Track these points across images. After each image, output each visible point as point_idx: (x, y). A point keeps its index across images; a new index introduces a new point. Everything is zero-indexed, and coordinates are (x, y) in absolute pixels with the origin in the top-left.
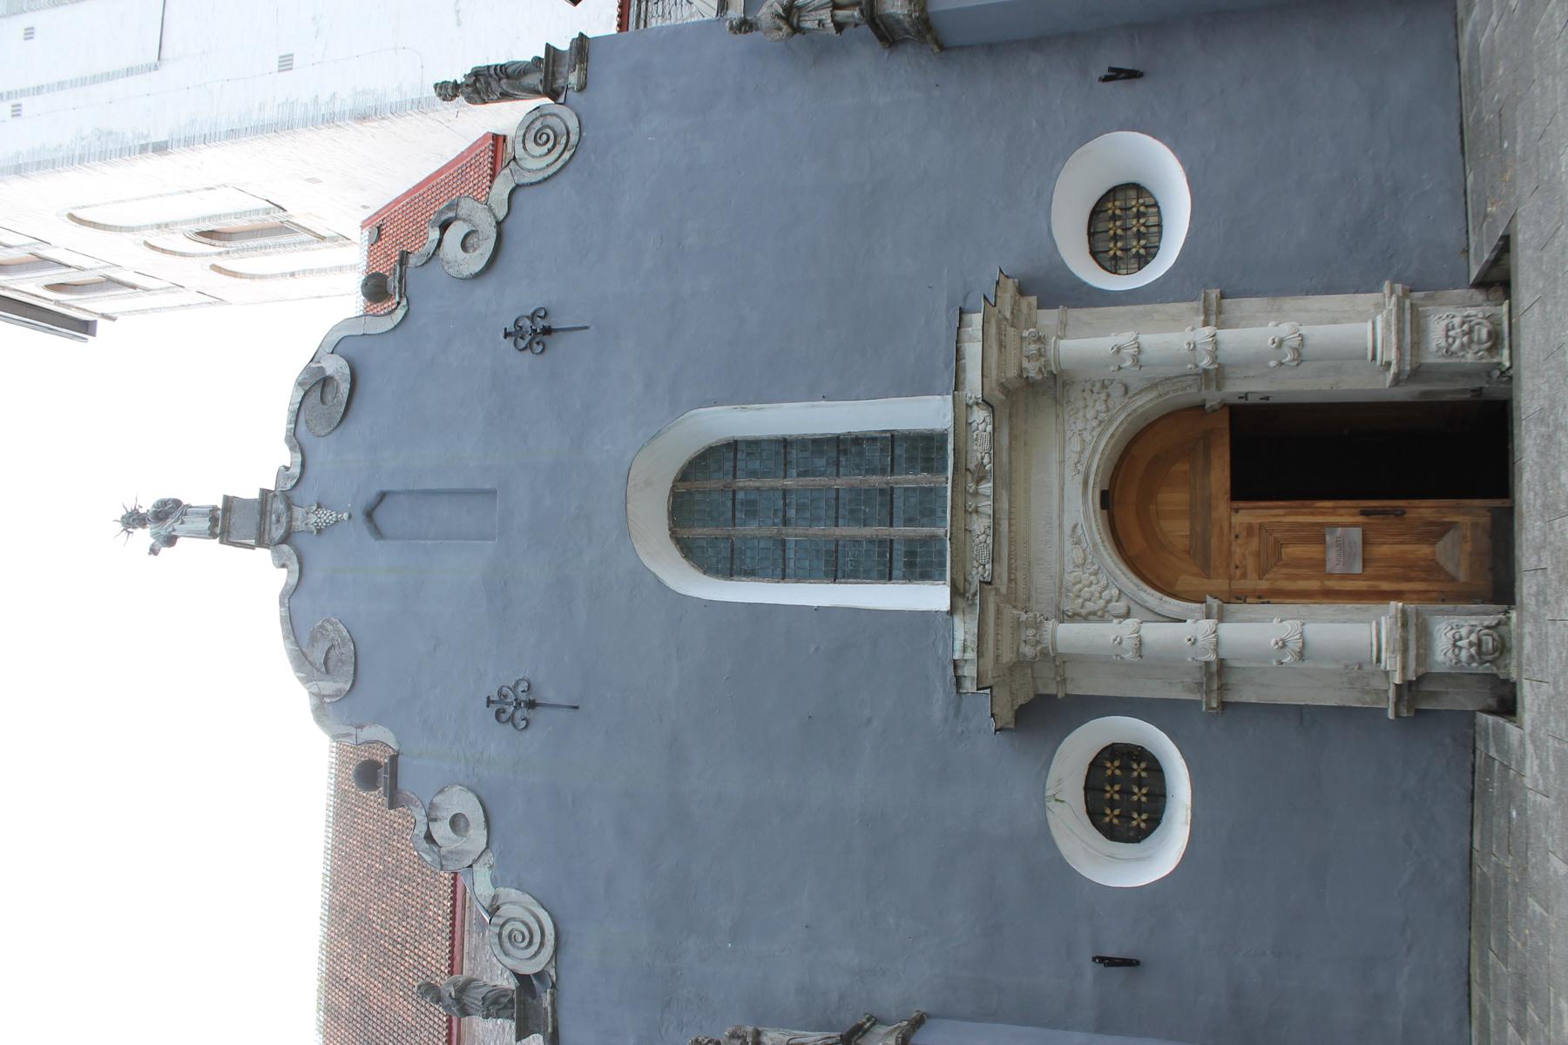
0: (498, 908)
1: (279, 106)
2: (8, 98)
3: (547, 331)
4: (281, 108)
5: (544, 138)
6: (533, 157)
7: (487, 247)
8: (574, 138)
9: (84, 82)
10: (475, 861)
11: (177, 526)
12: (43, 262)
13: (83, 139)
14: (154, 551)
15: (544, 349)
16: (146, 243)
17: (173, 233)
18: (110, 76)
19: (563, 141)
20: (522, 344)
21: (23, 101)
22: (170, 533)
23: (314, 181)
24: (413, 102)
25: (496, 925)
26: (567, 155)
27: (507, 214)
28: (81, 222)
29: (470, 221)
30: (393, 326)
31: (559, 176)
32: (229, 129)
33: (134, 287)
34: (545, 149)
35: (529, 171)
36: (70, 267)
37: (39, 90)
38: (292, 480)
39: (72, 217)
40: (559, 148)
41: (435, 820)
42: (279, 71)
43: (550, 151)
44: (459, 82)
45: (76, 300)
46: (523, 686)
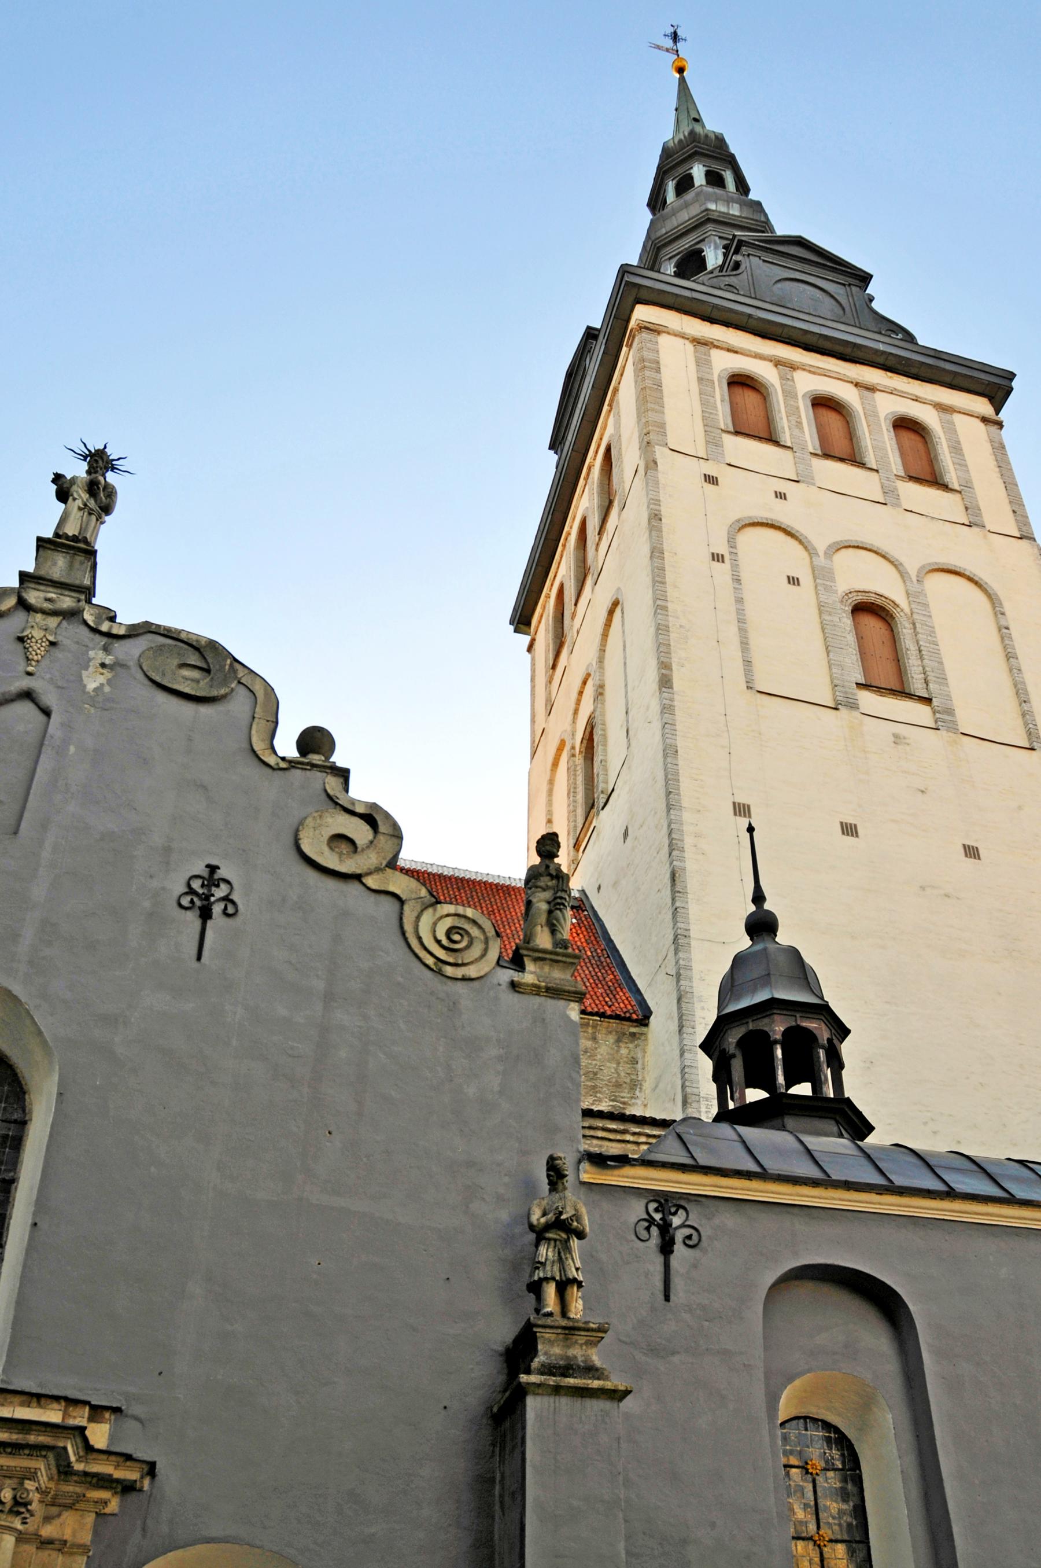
5: (456, 937)
6: (435, 924)
7: (330, 860)
8: (449, 970)
9: (741, 621)
16: (588, 675)
17: (595, 700)
18: (745, 645)
21: (727, 566)
23: (626, 834)
24: (686, 930)
26: (430, 961)
27: (369, 889)
28: (611, 612)
30: (256, 750)
31: (407, 950)
32: (678, 749)
33: (554, 667)
34: (441, 936)
35: (418, 918)
36: (576, 604)
40: (441, 954)
42: (734, 803)
43: (438, 942)
45: (549, 613)
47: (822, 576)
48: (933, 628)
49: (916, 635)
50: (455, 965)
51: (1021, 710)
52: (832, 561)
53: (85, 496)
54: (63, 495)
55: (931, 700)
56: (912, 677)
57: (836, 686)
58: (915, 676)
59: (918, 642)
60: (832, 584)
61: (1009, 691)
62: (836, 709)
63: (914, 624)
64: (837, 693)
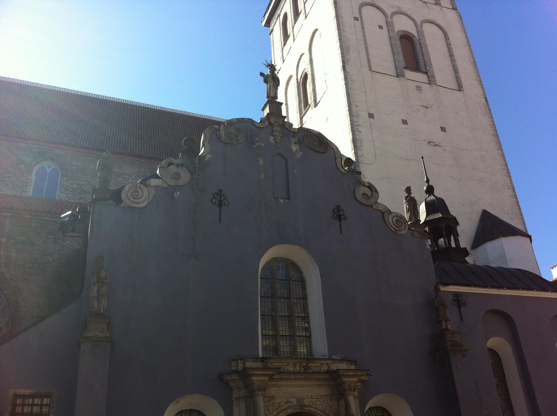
0: (146, 187)
1: (357, 112)
2: (360, 17)
3: (340, 220)
7: (364, 201)
10: (163, 180)
11: (272, 84)
12: (297, 14)
13: (347, 40)
14: (262, 74)
15: (333, 218)
16: (303, 54)
18: (367, 53)
19: (397, 229)
20: (336, 211)
25: (140, 185)
26: (393, 230)
30: (338, 167)
35: (388, 218)
37: (363, 28)
38: (289, 128)
39: (316, 30)
40: (396, 228)
41: (178, 167)
42: (368, 113)
43: (394, 224)
46: (227, 203)
47: (390, 25)
48: (427, 45)
49: (421, 48)
50: (399, 231)
52: (393, 19)
53: (273, 82)
54: (266, 81)
55: (427, 73)
59: (422, 50)
60: (394, 29)
61: (451, 68)
62: (397, 77)
63: (420, 44)
64: (398, 71)
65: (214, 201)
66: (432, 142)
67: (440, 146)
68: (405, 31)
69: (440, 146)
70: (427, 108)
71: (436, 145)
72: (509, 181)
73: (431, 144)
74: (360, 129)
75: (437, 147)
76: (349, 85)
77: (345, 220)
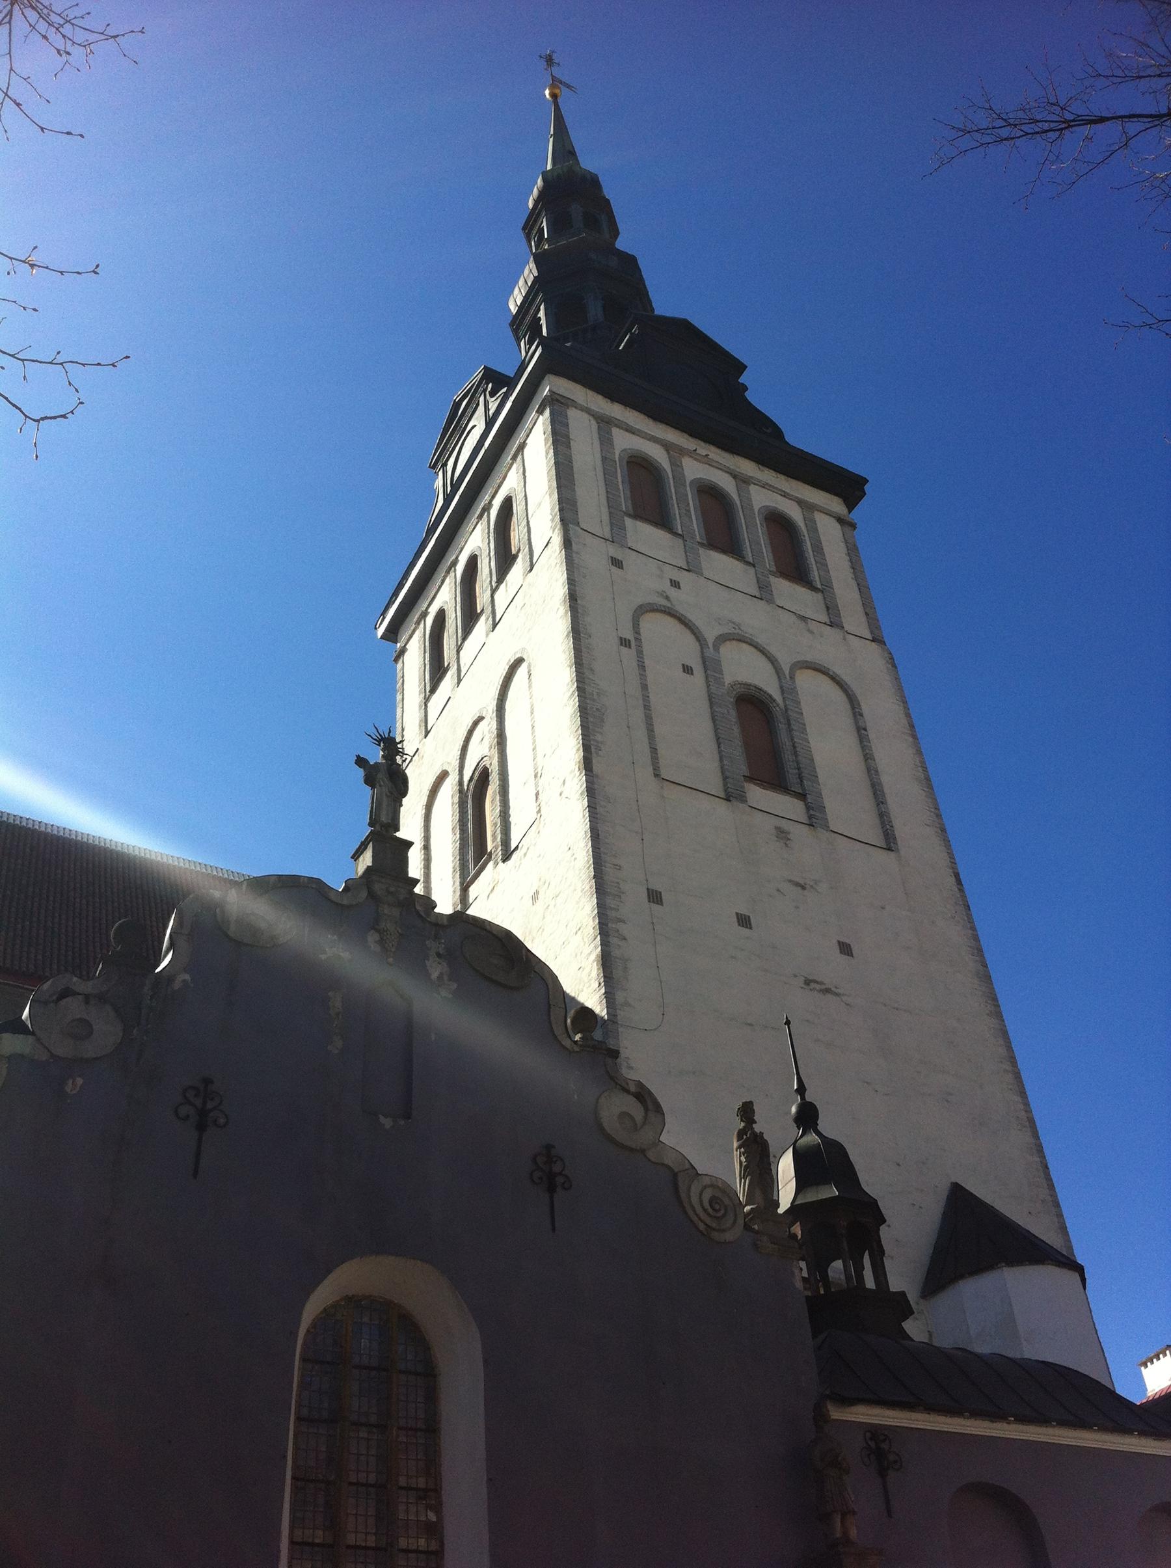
1: (618, 883)
2: (636, 639)
3: (551, 1189)
4: (616, 885)
9: (647, 707)
11: (385, 790)
12: (470, 617)
13: (598, 694)
14: (361, 762)
15: (533, 1181)
16: (481, 719)
19: (714, 1225)
22: (379, 782)
23: (535, 897)
24: (614, 1015)
26: (702, 1227)
29: (644, 1123)
37: (642, 667)
39: (519, 662)
40: (708, 1220)
41: (87, 1002)
42: (648, 889)
43: (705, 1210)
44: (754, 1126)
46: (222, 1121)
47: (711, 667)
48: (805, 725)
49: (790, 731)
50: (718, 1231)
51: (878, 810)
52: (719, 653)
54: (370, 781)
55: (805, 795)
56: (788, 772)
57: (727, 778)
58: (791, 771)
60: (721, 676)
62: (728, 800)
63: (789, 720)
64: (729, 785)
65: (183, 1111)
66: (815, 982)
67: (837, 994)
68: (750, 685)
69: (837, 994)
70: (803, 888)
71: (827, 991)
72: (1022, 1107)
73: (813, 985)
74: (624, 929)
75: (829, 996)
76: (600, 810)
77: (566, 1189)
